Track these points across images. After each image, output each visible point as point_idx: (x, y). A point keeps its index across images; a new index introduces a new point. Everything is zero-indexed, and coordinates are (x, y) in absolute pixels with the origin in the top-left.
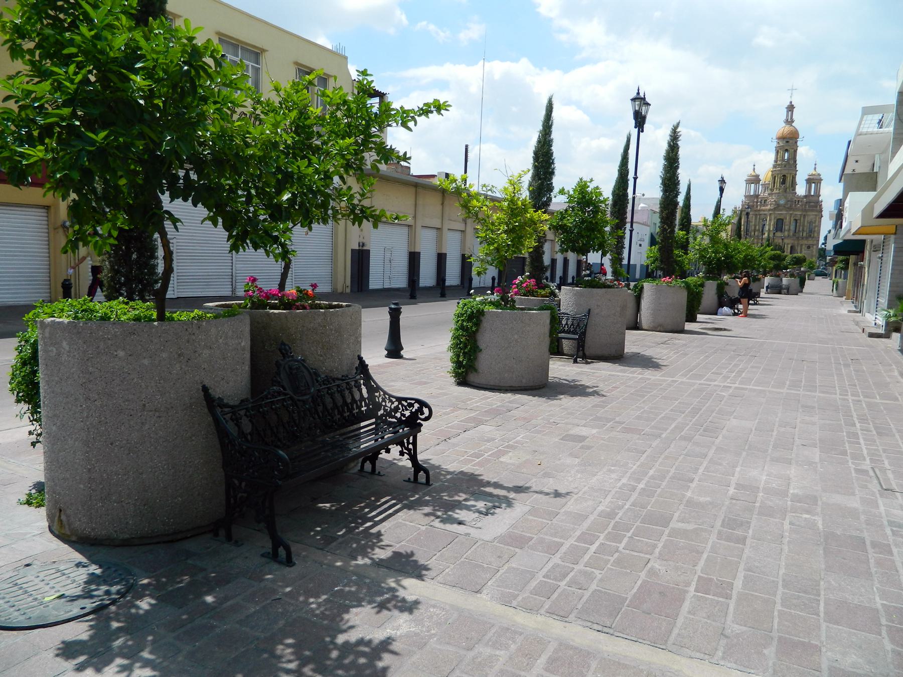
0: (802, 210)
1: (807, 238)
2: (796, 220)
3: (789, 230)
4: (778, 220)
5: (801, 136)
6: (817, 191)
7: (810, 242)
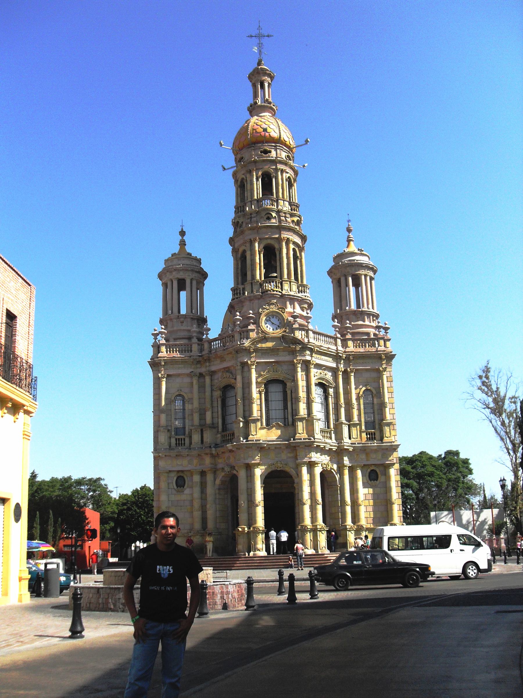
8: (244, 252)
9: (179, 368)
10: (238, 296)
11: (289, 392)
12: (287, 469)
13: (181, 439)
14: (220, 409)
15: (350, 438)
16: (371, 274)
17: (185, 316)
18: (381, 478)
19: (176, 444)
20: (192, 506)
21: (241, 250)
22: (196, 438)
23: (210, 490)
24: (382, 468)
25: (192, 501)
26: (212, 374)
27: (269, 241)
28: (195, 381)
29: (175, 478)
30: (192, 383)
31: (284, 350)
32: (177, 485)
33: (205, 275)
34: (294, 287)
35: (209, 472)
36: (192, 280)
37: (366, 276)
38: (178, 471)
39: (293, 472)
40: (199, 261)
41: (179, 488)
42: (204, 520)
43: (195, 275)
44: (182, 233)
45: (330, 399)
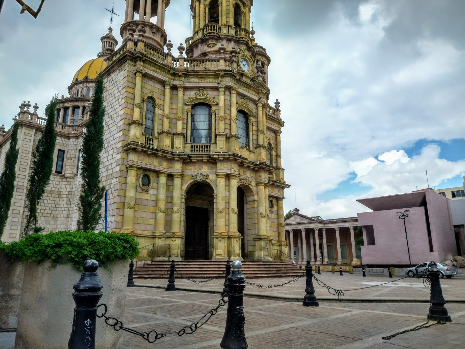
9: (156, 72)
10: (215, 31)
11: (251, 124)
12: (250, 186)
13: (150, 139)
18: (275, 208)
19: (145, 143)
25: (157, 201)
26: (186, 89)
29: (142, 176)
35: (179, 176)
39: (254, 189)
41: (144, 186)
42: (168, 223)
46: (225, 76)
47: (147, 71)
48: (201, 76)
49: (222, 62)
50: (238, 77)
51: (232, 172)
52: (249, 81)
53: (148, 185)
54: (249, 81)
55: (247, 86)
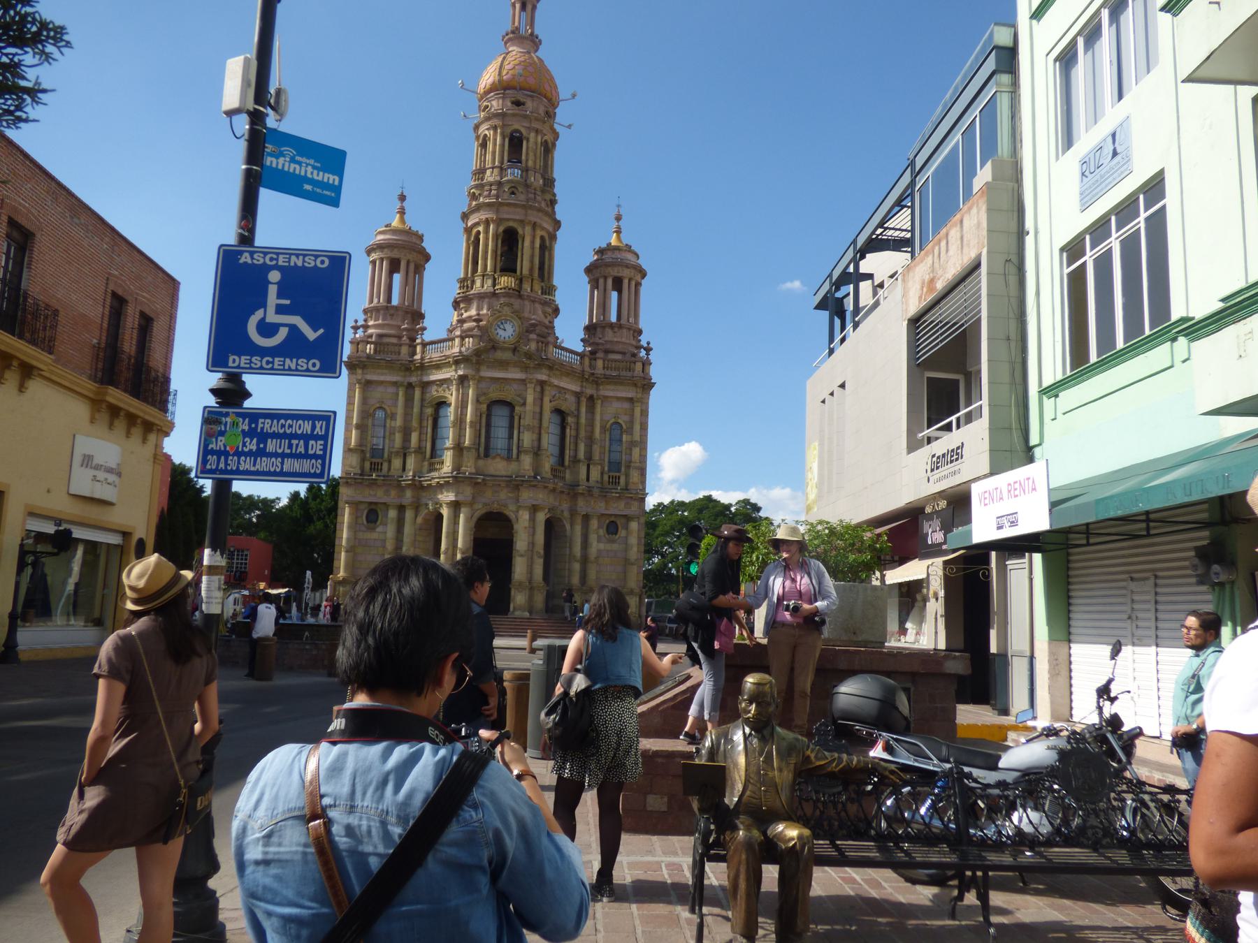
0: (582, 377)
1: (604, 493)
2: (559, 412)
3: (537, 452)
4: (493, 404)
5: (564, 91)
6: (631, 307)
7: (618, 508)
8: (478, 233)
11: (516, 418)
14: (430, 430)
15: (588, 480)
16: (638, 277)
17: (396, 308)
18: (622, 533)
20: (384, 547)
21: (474, 231)
22: (397, 463)
23: (408, 529)
24: (623, 520)
25: (384, 541)
26: (426, 385)
27: (511, 224)
28: (401, 394)
30: (397, 394)
31: (516, 364)
32: (368, 521)
33: (427, 258)
34: (537, 287)
36: (408, 262)
37: (630, 280)
38: (371, 503)
39: (512, 516)
40: (421, 238)
43: (412, 256)
44: (402, 198)
45: (568, 430)
46: (457, 362)
47: (369, 377)
48: (438, 367)
49: (457, 341)
50: (474, 359)
51: (461, 498)
52: (507, 355)
53: (376, 521)
54: (507, 355)
55: (503, 364)
